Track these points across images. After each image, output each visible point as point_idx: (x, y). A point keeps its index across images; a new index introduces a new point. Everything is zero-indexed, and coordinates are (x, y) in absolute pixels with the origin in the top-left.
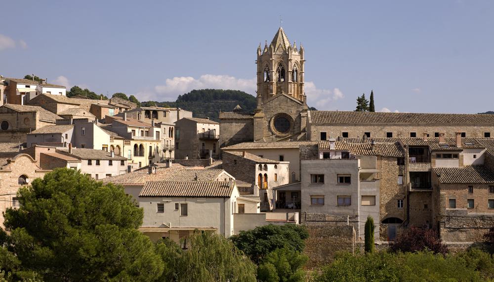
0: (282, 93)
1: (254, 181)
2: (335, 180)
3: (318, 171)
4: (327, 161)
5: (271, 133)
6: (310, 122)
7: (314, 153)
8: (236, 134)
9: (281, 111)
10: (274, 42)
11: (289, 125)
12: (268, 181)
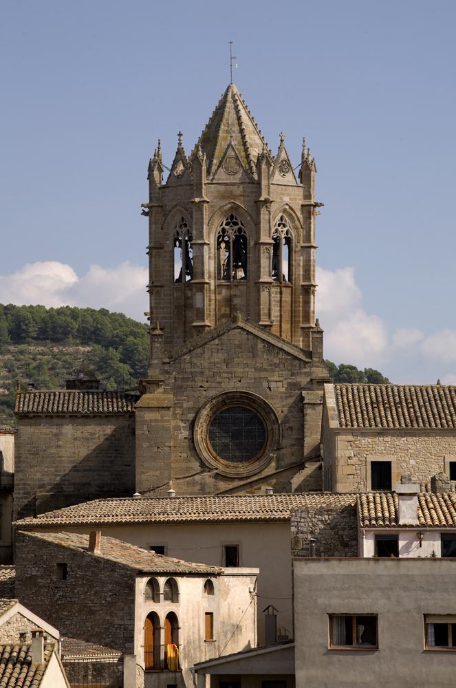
0: (235, 320)
1: (131, 639)
2: (418, 639)
3: (357, 602)
4: (387, 567)
5: (196, 465)
6: (334, 424)
7: (340, 538)
8: (75, 469)
9: (231, 386)
10: (209, 139)
11: (263, 434)
12: (181, 641)
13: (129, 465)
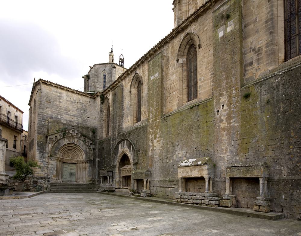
13: (89, 118)
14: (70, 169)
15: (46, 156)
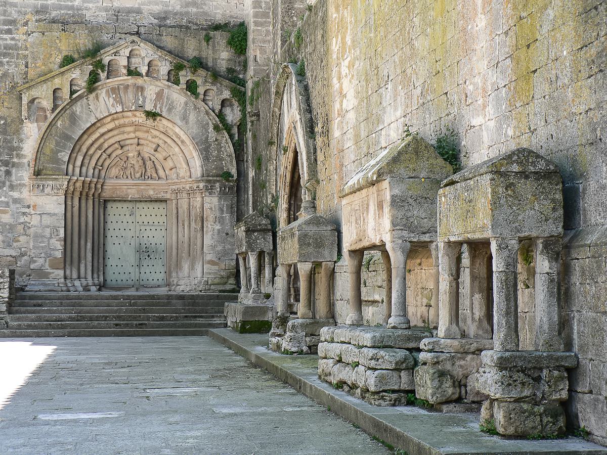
14: (138, 228)
15: (21, 178)
